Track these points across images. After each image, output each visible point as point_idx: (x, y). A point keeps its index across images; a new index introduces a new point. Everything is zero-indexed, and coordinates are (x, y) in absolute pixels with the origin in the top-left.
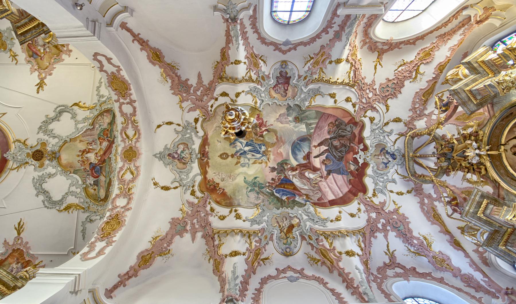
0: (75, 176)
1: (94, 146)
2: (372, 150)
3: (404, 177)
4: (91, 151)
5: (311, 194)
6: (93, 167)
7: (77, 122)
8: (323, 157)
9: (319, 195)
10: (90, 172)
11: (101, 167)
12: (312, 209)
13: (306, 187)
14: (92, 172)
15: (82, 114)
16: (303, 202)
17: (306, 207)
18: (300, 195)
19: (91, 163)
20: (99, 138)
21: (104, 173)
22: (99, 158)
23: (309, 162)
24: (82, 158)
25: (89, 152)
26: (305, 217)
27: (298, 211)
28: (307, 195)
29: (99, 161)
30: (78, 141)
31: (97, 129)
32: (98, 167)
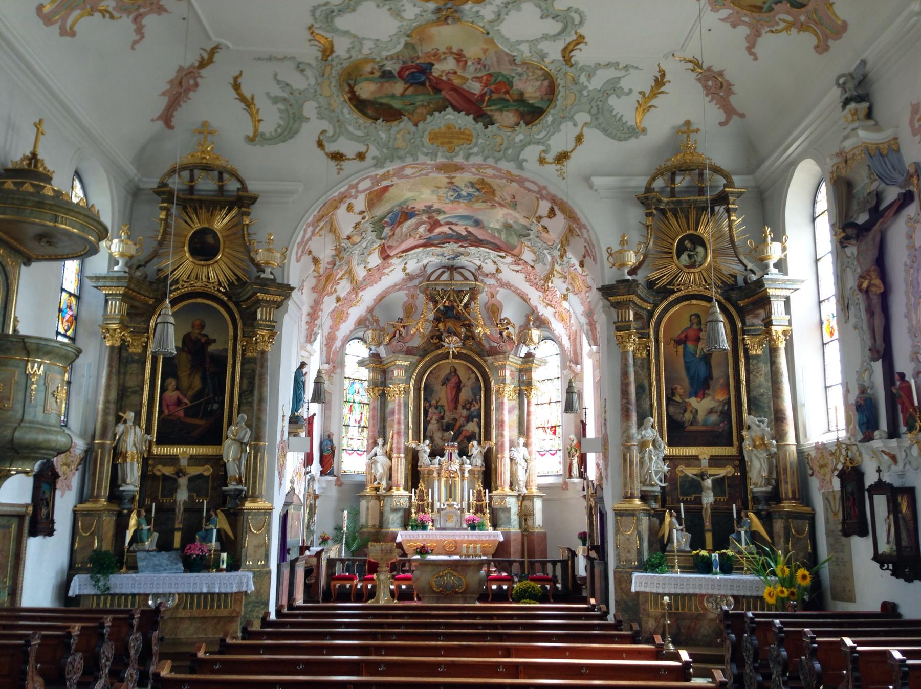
0: (400, 47)
1: (472, 69)
2: (462, 249)
3: (425, 267)
4: (461, 64)
5: (395, 237)
6: (425, 69)
7: (533, 43)
8: (450, 232)
9: (394, 244)
10: (410, 64)
11: (423, 84)
12: (376, 245)
13: (404, 229)
14: (412, 67)
15: (554, 52)
16: (383, 235)
17: (378, 241)
18: (392, 229)
19: (433, 65)
20: (491, 75)
21: (411, 90)
22: (444, 78)
23: (441, 225)
24: (444, 53)
25: (458, 61)
26: (364, 245)
27: (371, 236)
28: (394, 234)
29: (439, 79)
30: (485, 47)
31: (513, 70)
32: (423, 78)
